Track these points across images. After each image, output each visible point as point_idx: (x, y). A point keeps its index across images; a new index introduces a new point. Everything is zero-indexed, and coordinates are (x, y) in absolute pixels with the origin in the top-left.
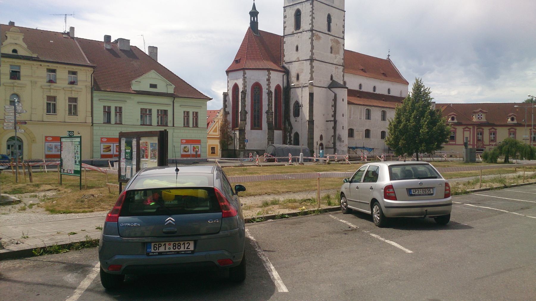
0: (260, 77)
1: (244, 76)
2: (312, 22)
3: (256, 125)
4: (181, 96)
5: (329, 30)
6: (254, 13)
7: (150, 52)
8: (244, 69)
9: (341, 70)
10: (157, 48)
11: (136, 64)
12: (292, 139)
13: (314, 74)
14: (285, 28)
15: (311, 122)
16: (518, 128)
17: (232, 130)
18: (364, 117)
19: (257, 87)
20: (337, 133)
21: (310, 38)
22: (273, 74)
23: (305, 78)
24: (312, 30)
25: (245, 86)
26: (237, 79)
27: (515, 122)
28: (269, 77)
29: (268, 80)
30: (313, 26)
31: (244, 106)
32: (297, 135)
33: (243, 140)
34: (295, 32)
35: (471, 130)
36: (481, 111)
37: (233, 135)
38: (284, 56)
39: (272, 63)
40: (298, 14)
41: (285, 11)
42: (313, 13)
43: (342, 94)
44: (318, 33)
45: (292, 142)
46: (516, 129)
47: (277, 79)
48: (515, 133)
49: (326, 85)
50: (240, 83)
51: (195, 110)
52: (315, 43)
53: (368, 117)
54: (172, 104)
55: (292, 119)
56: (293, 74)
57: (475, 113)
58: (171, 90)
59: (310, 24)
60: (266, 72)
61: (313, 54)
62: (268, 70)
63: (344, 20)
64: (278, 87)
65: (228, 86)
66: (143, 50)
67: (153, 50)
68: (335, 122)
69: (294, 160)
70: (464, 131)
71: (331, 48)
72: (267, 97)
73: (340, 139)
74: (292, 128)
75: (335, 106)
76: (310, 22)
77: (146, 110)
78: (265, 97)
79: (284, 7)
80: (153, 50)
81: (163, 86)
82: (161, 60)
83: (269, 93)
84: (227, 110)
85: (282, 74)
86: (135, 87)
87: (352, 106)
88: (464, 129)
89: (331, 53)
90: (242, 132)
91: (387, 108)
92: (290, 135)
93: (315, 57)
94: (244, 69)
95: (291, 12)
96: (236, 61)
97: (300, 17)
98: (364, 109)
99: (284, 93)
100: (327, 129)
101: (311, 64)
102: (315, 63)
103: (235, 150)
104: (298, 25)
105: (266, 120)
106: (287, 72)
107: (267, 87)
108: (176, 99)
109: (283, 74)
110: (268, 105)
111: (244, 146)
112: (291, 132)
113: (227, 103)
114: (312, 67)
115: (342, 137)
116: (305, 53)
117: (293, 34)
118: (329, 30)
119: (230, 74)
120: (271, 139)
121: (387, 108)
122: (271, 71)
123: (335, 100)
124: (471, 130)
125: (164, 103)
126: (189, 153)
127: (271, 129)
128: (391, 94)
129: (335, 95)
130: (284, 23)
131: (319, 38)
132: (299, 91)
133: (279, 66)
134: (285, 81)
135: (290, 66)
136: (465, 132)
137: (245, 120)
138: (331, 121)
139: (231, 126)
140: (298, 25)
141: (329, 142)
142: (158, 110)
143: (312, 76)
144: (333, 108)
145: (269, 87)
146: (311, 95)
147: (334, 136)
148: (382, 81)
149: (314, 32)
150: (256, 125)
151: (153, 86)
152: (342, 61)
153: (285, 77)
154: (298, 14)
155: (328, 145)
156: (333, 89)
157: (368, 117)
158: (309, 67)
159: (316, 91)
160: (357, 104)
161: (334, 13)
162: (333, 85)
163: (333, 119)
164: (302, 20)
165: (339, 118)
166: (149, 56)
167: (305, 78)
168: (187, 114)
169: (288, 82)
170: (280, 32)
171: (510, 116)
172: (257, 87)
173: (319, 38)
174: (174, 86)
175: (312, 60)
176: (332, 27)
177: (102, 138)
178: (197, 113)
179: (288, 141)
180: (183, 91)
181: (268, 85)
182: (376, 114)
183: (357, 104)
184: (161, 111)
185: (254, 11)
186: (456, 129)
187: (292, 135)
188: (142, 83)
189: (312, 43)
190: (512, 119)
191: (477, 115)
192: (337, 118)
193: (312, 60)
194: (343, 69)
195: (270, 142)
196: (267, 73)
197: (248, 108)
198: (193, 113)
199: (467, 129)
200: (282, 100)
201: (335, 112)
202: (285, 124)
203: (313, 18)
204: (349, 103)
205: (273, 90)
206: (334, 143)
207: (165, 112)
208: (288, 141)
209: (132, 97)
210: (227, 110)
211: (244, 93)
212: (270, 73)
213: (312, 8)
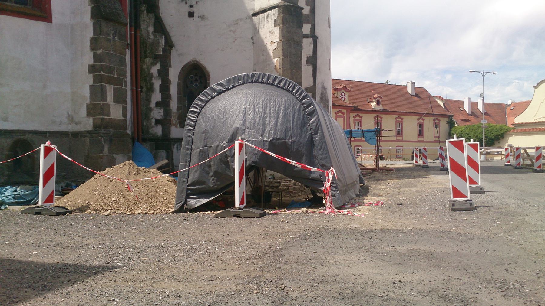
12: (174, 90)
16: (382, 116)
27: (381, 107)
35: (345, 116)
36: (345, 88)
74: (170, 45)
92: (164, 74)
112: (165, 62)
124: (345, 116)
171: (375, 98)
179: (157, 97)
187: (174, 75)
190: (378, 103)
191: (339, 93)
195: (110, 91)
199: (340, 114)
202: (136, 24)
208: (157, 97)
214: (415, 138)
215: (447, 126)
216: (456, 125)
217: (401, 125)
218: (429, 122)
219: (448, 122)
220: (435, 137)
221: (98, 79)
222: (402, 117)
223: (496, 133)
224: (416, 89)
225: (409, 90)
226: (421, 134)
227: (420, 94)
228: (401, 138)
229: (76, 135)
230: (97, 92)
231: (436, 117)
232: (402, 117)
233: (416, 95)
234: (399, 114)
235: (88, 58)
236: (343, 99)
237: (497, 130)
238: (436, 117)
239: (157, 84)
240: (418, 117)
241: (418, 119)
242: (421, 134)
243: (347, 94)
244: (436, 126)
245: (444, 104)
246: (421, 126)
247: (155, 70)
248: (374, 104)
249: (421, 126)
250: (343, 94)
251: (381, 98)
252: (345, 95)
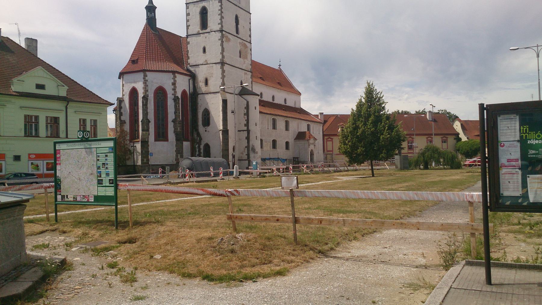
0: (164, 80)
1: (144, 78)
2: (222, 22)
3: (161, 136)
4: (76, 99)
5: (237, 32)
6: (151, 9)
7: (28, 46)
8: (144, 71)
9: (250, 76)
10: (36, 40)
11: (11, 59)
12: (202, 151)
13: (225, 79)
14: (188, 27)
15: (225, 132)
17: (131, 142)
18: (271, 126)
19: (161, 92)
20: (251, 143)
21: (219, 40)
22: (179, 78)
23: (215, 84)
24: (221, 31)
25: (146, 91)
26: (135, 82)
28: (175, 81)
29: (174, 84)
30: (222, 26)
31: (145, 114)
32: (207, 146)
33: (145, 153)
34: (201, 32)
37: (132, 149)
38: (188, 58)
39: (175, 66)
40: (204, 12)
41: (187, 8)
42: (222, 12)
43: (254, 101)
44: (228, 34)
45: (202, 155)
46: (447, 138)
47: (183, 84)
48: (431, 141)
49: (237, 92)
50: (140, 87)
51: (94, 118)
52: (225, 44)
53: (274, 127)
54: (64, 109)
55: (201, 129)
56: (201, 78)
58: (63, 92)
59: (219, 24)
60: (171, 75)
61: (223, 57)
62: (174, 72)
63: (250, 23)
64: (184, 92)
65: (123, 91)
66: (17, 42)
67: (32, 42)
68: (248, 131)
69: (225, 174)
71: (240, 52)
72: (173, 104)
73: (254, 150)
75: (247, 114)
76: (220, 22)
77: (31, 116)
78: (170, 103)
79: (186, 4)
80: (32, 42)
81: (52, 88)
82: (42, 54)
83: (176, 99)
84: (123, 118)
85: (187, 78)
86: (16, 87)
87: (262, 114)
89: (240, 57)
90: (145, 144)
91: (289, 117)
92: (199, 147)
93: (226, 60)
94: (144, 71)
95: (196, 10)
96: (133, 61)
97: (207, 16)
98: (270, 118)
99: (191, 100)
100: (240, 139)
101: (222, 68)
102: (226, 67)
103: (135, 166)
104: (204, 24)
105: (173, 129)
106: (193, 77)
107: (173, 92)
108: (71, 104)
109: (189, 78)
110: (175, 113)
111: (148, 160)
113: (122, 111)
114: (223, 71)
115: (255, 147)
116: (214, 55)
117: (198, 34)
118: (237, 32)
119: (126, 76)
120: (179, 151)
121: (289, 117)
122: (176, 75)
123: (247, 108)
125: (55, 109)
126: (41, 172)
127: (180, 139)
128: (287, 105)
129: (248, 102)
130: (188, 21)
131: (228, 40)
132: (208, 97)
133: (183, 68)
134: (191, 86)
135: (197, 69)
137: (148, 130)
138: (243, 131)
139: (128, 138)
140: (204, 24)
141: (242, 153)
142: (47, 117)
143: (223, 81)
144: (246, 117)
145: (175, 92)
146: (225, 102)
147: (248, 147)
148: (279, 91)
149: (224, 33)
150: (161, 136)
151: (41, 87)
152: (250, 67)
153: (191, 81)
154: (204, 12)
155: (241, 157)
156: (244, 96)
157: (274, 127)
158: (220, 71)
159: (229, 98)
160: (265, 113)
161: (242, 14)
162: (244, 92)
163: (245, 128)
164: (209, 19)
165: (252, 127)
166: (27, 51)
167: (215, 84)
168: (83, 122)
169: (195, 87)
170: (182, 32)
172: (161, 92)
173: (228, 40)
174: (66, 88)
175: (222, 63)
176: (237, 28)
177: (29, 154)
178: (95, 121)
179: (197, 153)
180: (77, 94)
181: (174, 89)
182: (281, 124)
183: (265, 113)
184: (51, 118)
185: (151, 5)
186: (413, 138)
187: (202, 147)
188: (26, 83)
189: (222, 45)
192: (250, 128)
193: (222, 63)
194: (252, 76)
196: (172, 76)
197: (151, 116)
198: (91, 120)
200: (189, 108)
201: (248, 121)
202: (193, 135)
203: (222, 17)
204: (260, 112)
205: (179, 95)
206: (248, 155)
207: (56, 120)
208: (197, 153)
209: (13, 100)
210: (123, 118)
211: (145, 98)
212: (175, 77)
213: (221, 6)
221: (177, 153)
223: (475, 147)
229: (173, 165)
230: (177, 156)
235: (175, 149)
239: (197, 150)
247: (197, 146)
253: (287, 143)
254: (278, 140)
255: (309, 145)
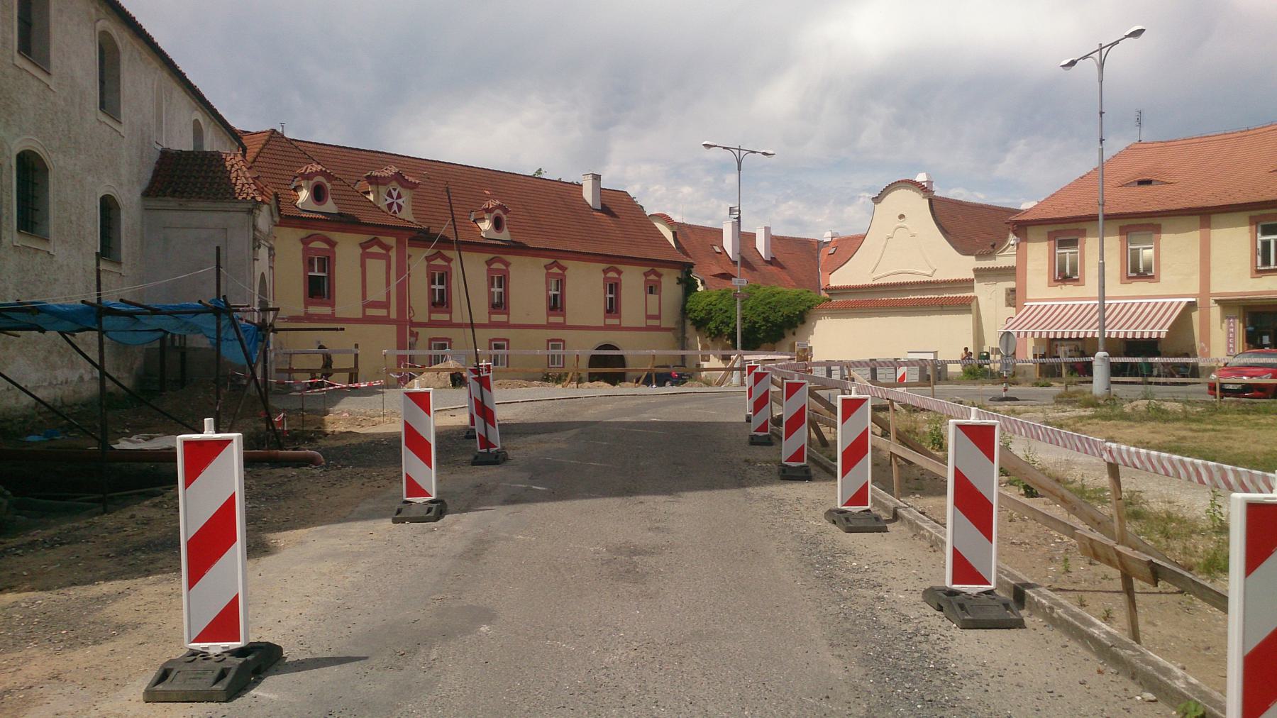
27: (505, 235)
35: (393, 254)
36: (398, 177)
57: (373, 180)
70: (365, 256)
88: (364, 246)
124: (393, 254)
136: (369, 262)
171: (488, 211)
190: (498, 224)
191: (383, 190)
199: (375, 249)
214: (598, 318)
215: (678, 290)
216: (700, 288)
217: (561, 283)
218: (632, 279)
219: (680, 281)
220: (648, 317)
222: (563, 263)
223: (786, 311)
224: (602, 193)
225: (588, 195)
226: (612, 308)
227: (616, 206)
228: (559, 320)
231: (654, 265)
232: (563, 263)
233: (605, 209)
234: (556, 257)
236: (395, 207)
237: (789, 303)
238: (654, 265)
240: (604, 266)
241: (605, 272)
242: (612, 308)
243: (404, 192)
244: (652, 289)
245: (675, 234)
246: (613, 287)
248: (486, 226)
249: (613, 287)
250: (395, 194)
251: (506, 211)
252: (399, 196)
253: (109, 207)
254: (57, 163)
255: (256, 245)
